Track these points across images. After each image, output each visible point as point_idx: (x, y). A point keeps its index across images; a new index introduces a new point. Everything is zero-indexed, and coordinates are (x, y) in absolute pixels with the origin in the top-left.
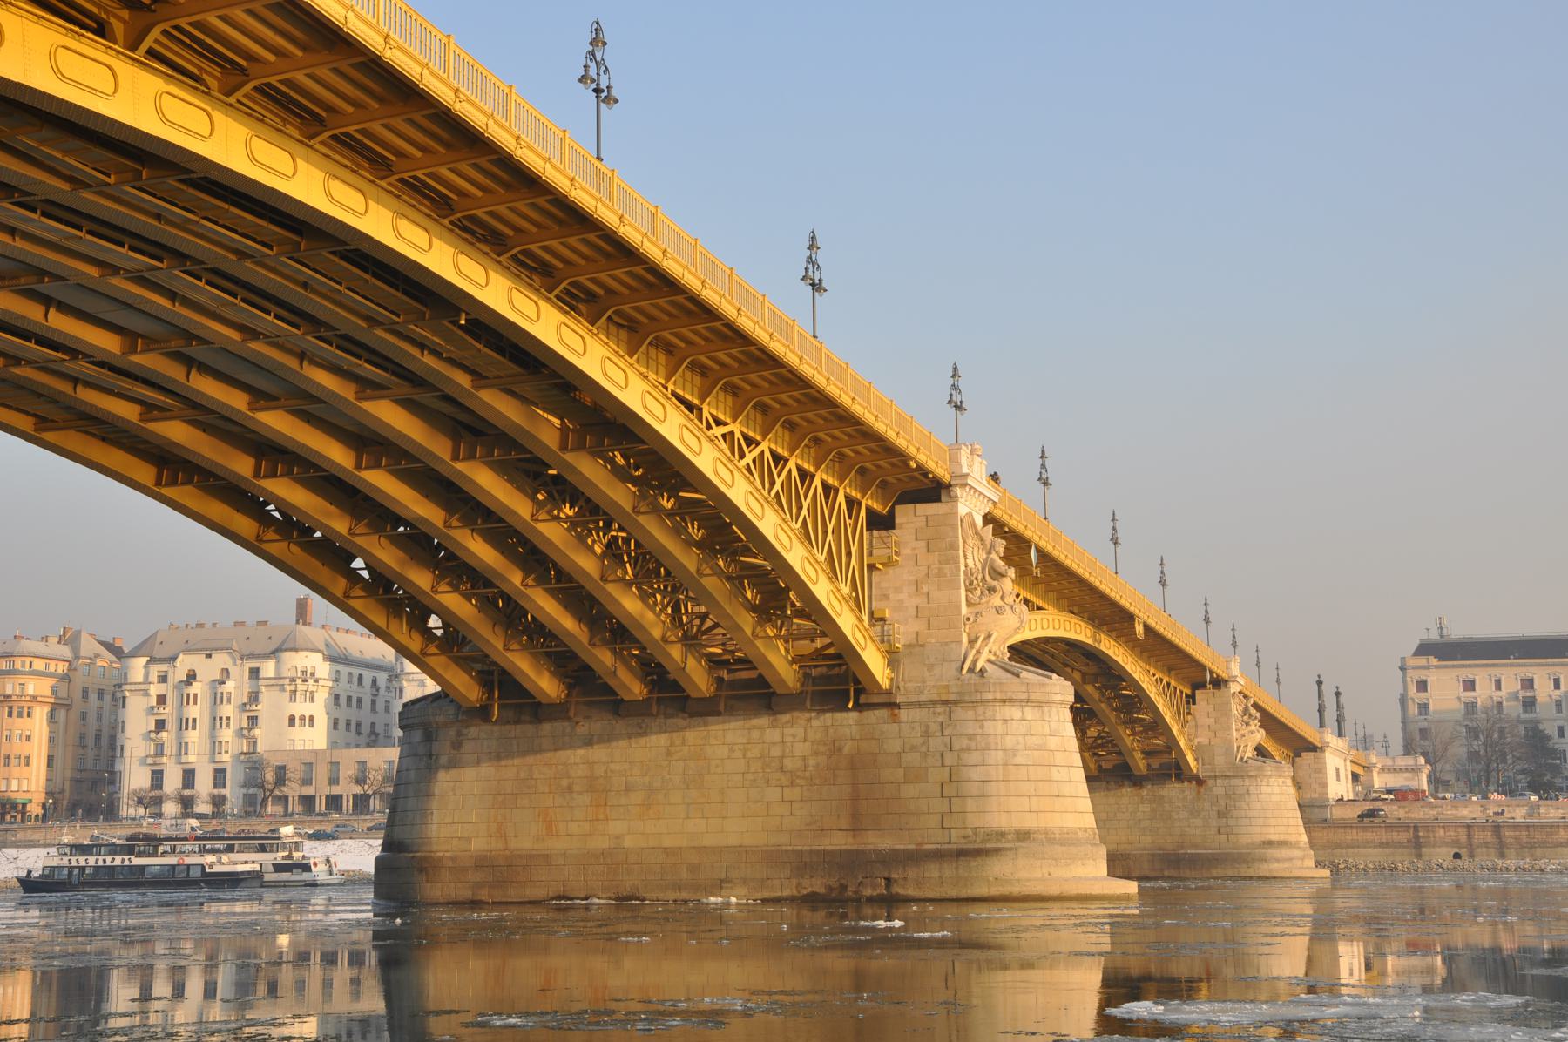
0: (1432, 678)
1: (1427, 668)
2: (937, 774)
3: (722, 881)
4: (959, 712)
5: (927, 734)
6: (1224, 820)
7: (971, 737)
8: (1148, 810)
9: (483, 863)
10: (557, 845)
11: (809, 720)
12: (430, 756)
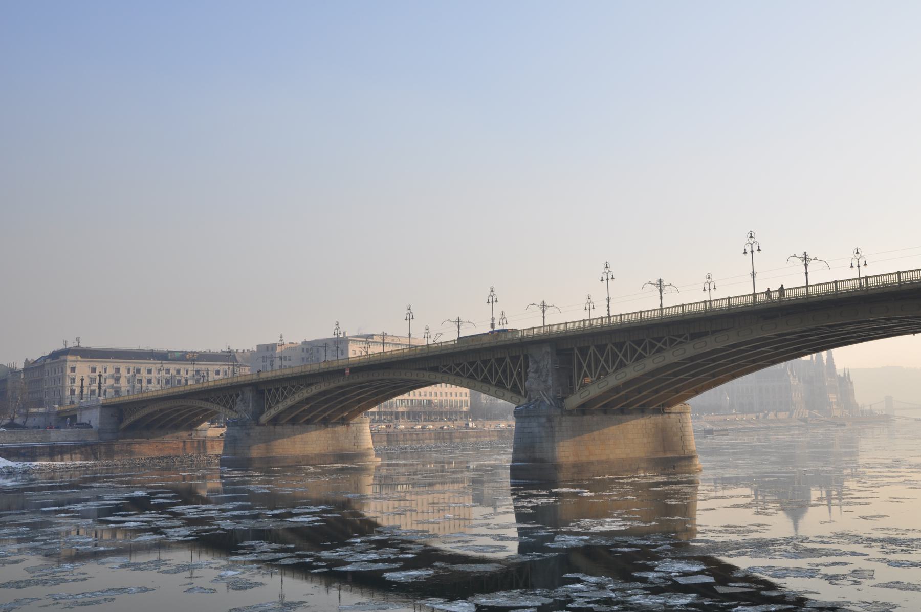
0: (78, 366)
1: (77, 361)
2: (680, 434)
3: (637, 469)
4: (682, 415)
5: (677, 422)
6: (356, 440)
7: (686, 423)
8: (330, 436)
9: (575, 465)
10: (593, 458)
11: (651, 417)
12: (552, 427)
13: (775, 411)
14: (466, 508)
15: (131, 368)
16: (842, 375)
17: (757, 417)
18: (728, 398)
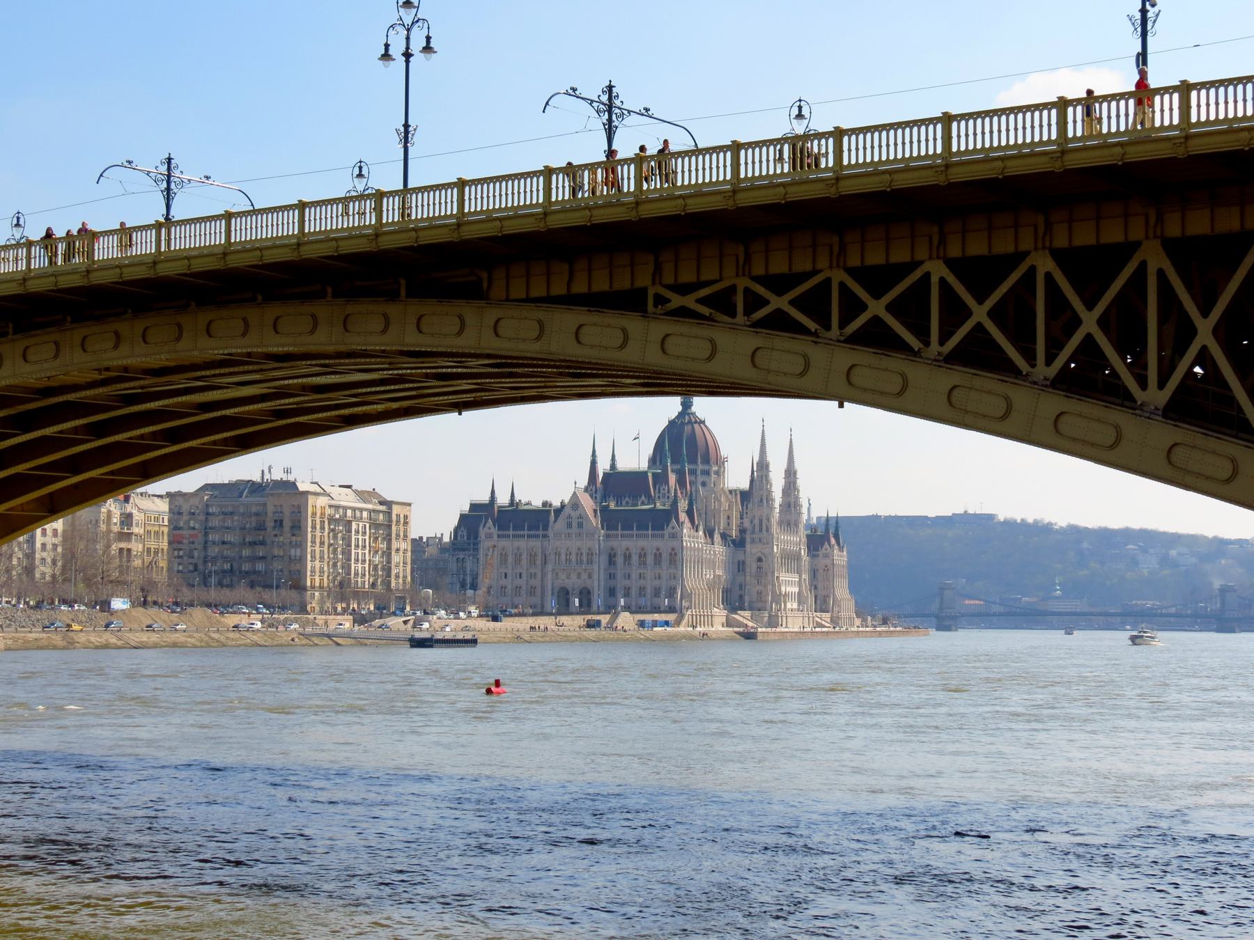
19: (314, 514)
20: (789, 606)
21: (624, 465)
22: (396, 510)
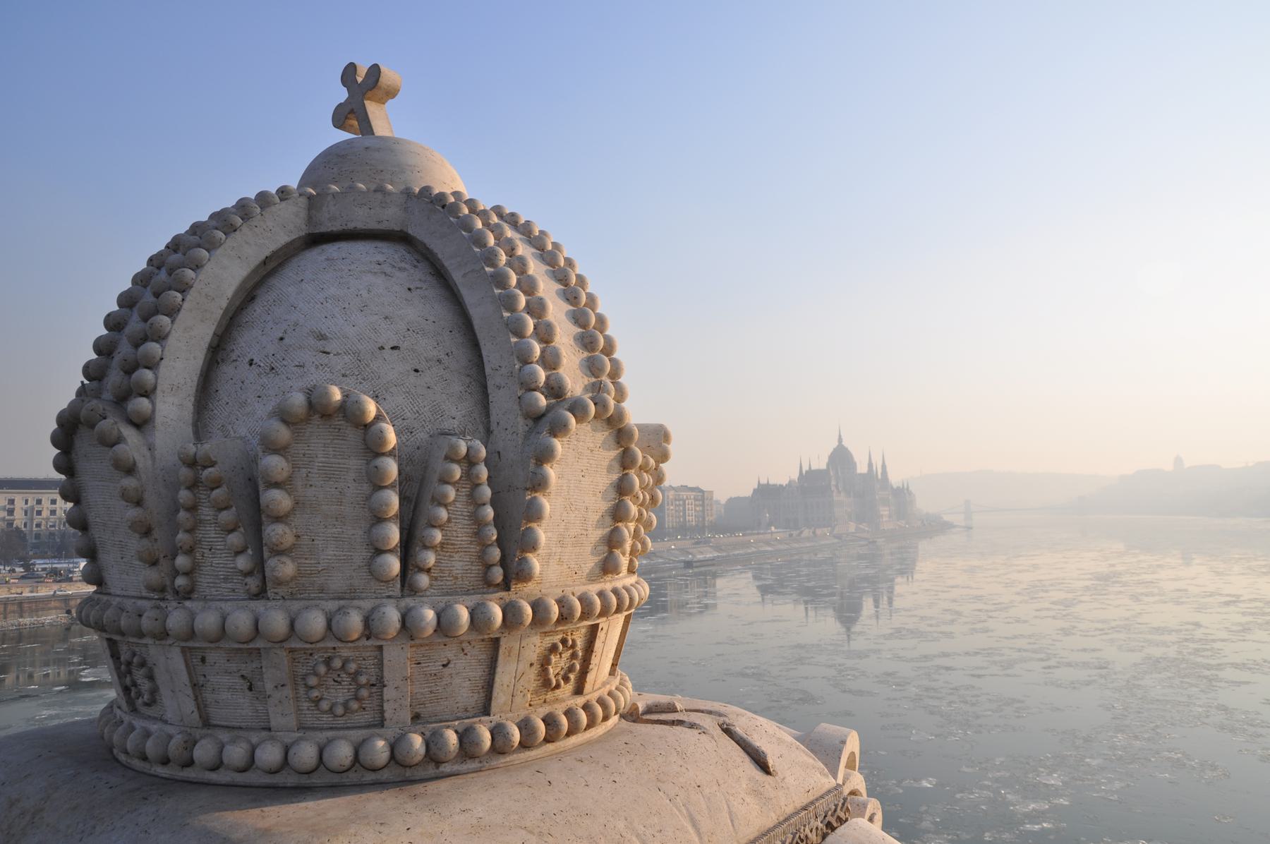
13: (813, 528)
14: (110, 709)
15: (30, 499)
16: (901, 487)
17: (791, 535)
18: (768, 515)
19: (668, 498)
20: (884, 520)
21: (813, 468)
22: (706, 494)
